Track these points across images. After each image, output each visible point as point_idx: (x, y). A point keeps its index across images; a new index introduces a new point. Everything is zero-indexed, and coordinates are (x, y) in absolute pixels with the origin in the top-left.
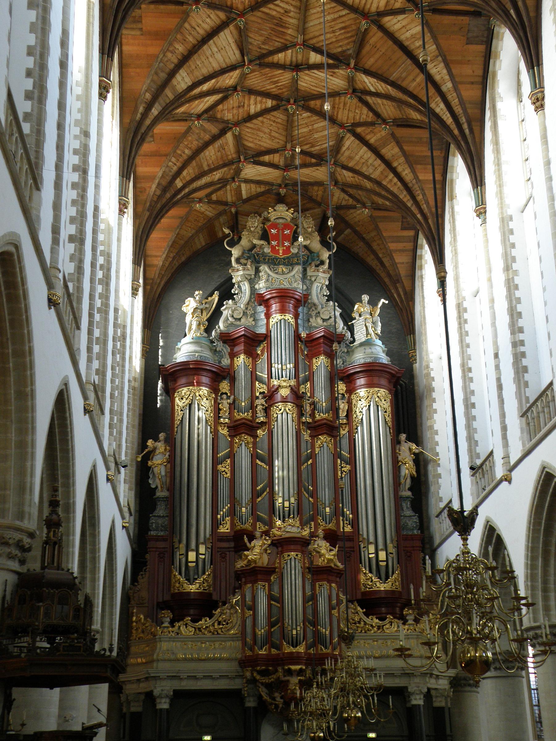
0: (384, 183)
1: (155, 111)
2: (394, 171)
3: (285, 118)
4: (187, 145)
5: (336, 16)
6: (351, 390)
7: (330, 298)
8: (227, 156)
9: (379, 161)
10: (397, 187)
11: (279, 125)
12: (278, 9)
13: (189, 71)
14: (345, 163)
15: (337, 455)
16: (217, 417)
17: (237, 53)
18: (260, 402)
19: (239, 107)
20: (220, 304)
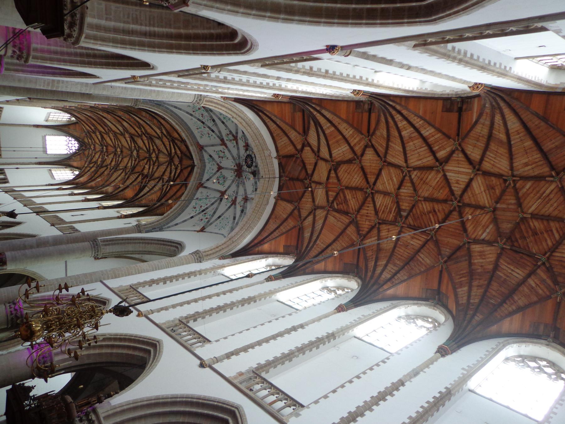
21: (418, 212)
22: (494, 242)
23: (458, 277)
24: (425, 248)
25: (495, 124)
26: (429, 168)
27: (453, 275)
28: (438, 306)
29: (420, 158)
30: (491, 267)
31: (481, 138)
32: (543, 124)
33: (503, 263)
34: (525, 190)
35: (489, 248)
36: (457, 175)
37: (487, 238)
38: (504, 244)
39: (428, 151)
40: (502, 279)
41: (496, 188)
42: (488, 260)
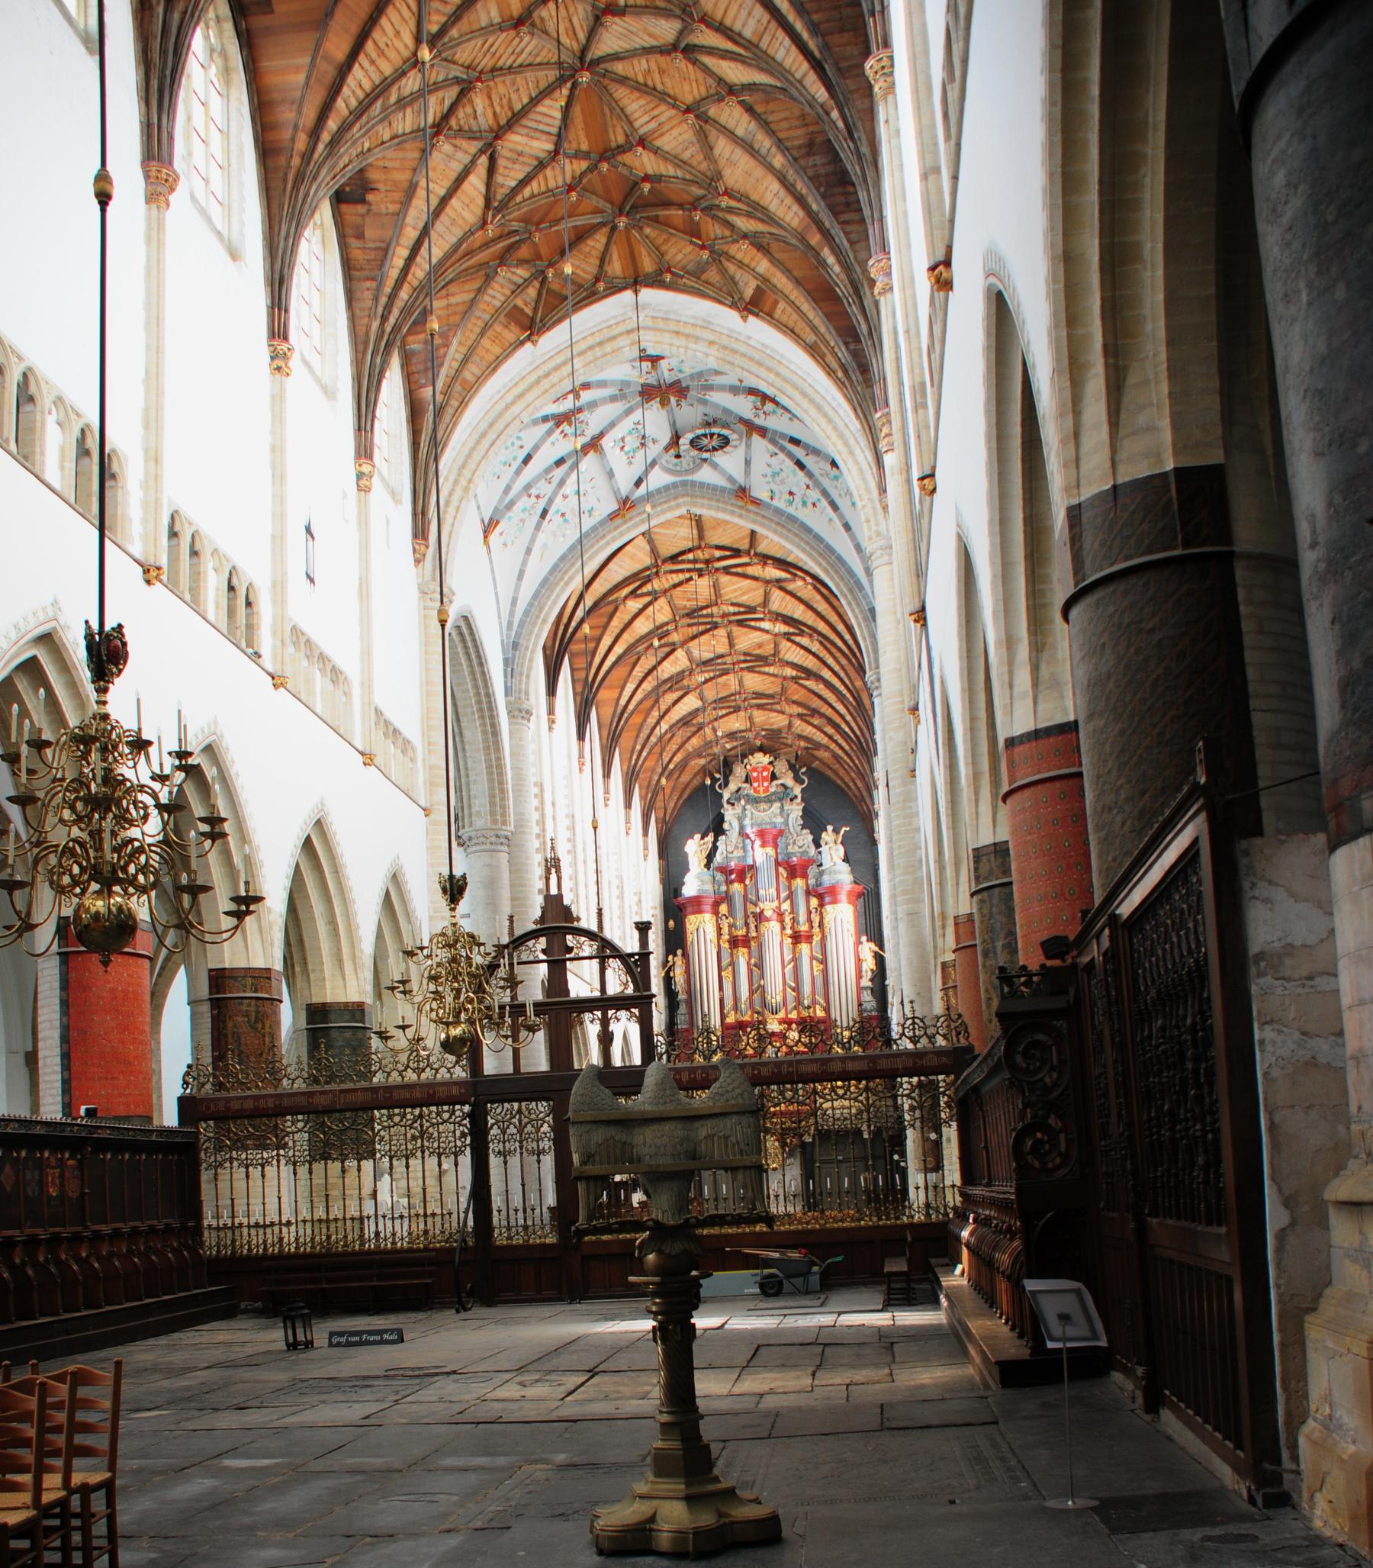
1: (644, 754)
2: (836, 742)
6: (822, 905)
7: (803, 827)
15: (812, 958)
16: (719, 935)
18: (751, 920)
20: (716, 840)
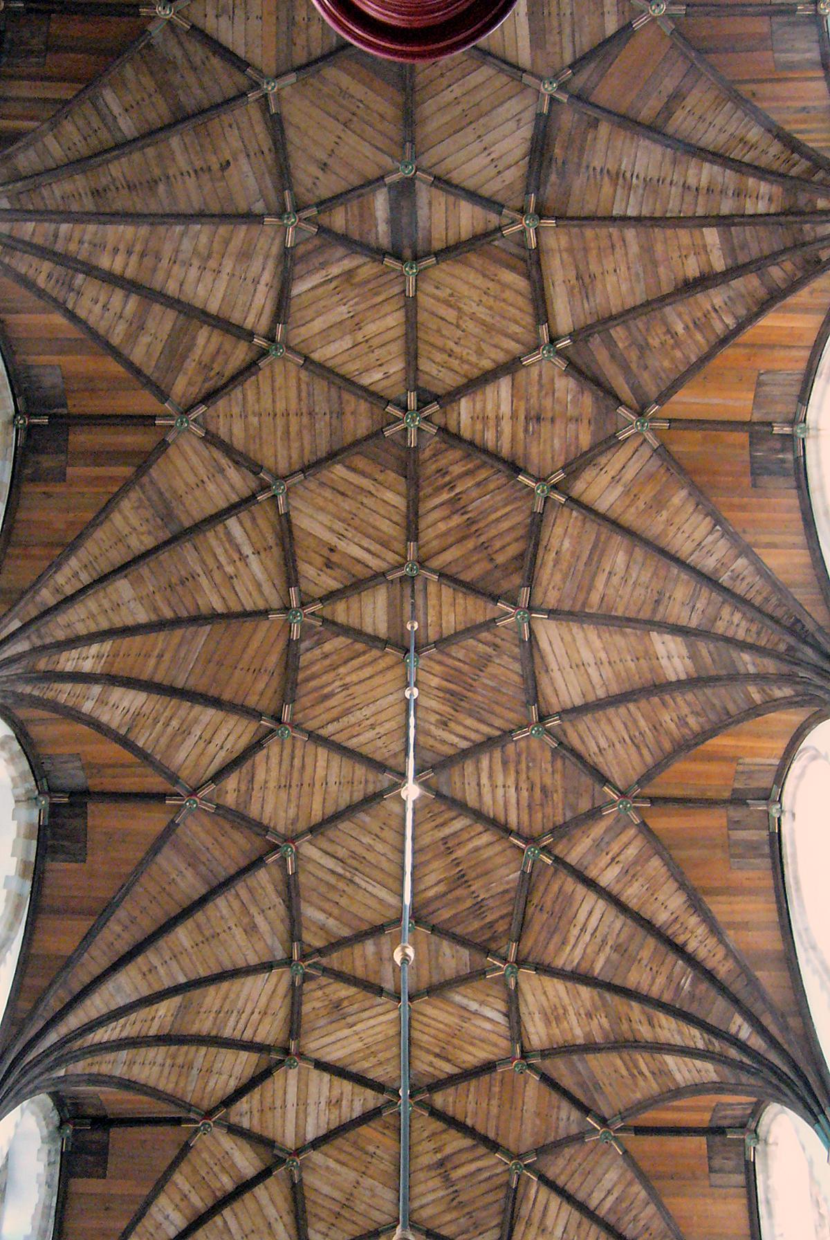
0: (144, 230)
2: (130, 286)
3: (424, 365)
4: (677, 344)
5: (345, 719)
8: (571, 250)
9: (172, 288)
10: (109, 247)
11: (439, 342)
12: (460, 730)
13: (655, 662)
14: (255, 229)
17: (544, 644)
19: (538, 419)
21: (454, 1215)
22: (506, 985)
23: (641, 1083)
24: (571, 1188)
25: (124, 1035)
26: (297, 1194)
27: (639, 1095)
28: (761, 1131)
29: (266, 1230)
30: (585, 991)
31: (180, 1061)
32: (121, 914)
33: (568, 958)
34: (331, 923)
35: (530, 998)
36: (312, 1109)
37: (502, 1006)
38: (505, 960)
39: (237, 1205)
40: (615, 956)
41: (335, 997)
42: (566, 1000)
